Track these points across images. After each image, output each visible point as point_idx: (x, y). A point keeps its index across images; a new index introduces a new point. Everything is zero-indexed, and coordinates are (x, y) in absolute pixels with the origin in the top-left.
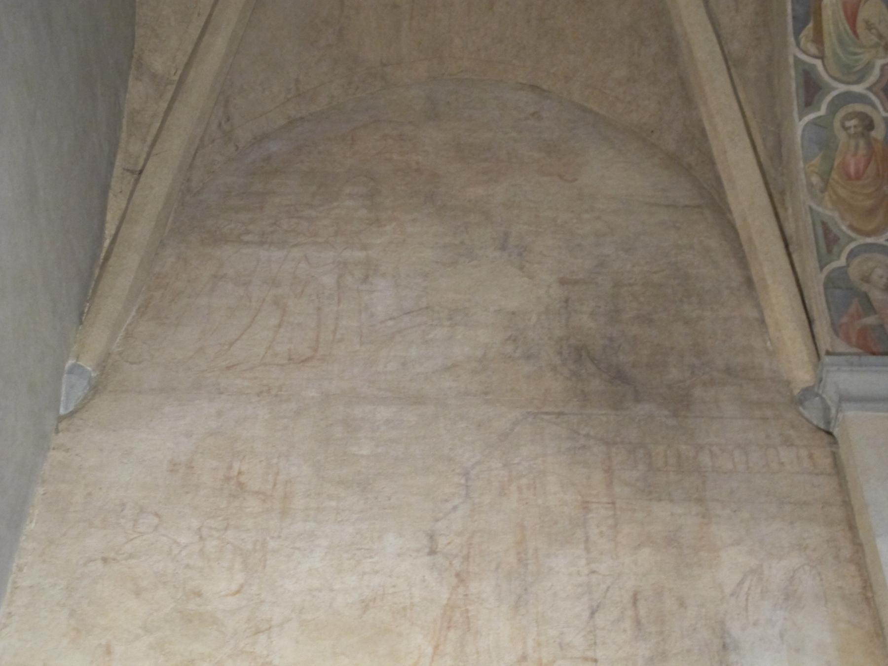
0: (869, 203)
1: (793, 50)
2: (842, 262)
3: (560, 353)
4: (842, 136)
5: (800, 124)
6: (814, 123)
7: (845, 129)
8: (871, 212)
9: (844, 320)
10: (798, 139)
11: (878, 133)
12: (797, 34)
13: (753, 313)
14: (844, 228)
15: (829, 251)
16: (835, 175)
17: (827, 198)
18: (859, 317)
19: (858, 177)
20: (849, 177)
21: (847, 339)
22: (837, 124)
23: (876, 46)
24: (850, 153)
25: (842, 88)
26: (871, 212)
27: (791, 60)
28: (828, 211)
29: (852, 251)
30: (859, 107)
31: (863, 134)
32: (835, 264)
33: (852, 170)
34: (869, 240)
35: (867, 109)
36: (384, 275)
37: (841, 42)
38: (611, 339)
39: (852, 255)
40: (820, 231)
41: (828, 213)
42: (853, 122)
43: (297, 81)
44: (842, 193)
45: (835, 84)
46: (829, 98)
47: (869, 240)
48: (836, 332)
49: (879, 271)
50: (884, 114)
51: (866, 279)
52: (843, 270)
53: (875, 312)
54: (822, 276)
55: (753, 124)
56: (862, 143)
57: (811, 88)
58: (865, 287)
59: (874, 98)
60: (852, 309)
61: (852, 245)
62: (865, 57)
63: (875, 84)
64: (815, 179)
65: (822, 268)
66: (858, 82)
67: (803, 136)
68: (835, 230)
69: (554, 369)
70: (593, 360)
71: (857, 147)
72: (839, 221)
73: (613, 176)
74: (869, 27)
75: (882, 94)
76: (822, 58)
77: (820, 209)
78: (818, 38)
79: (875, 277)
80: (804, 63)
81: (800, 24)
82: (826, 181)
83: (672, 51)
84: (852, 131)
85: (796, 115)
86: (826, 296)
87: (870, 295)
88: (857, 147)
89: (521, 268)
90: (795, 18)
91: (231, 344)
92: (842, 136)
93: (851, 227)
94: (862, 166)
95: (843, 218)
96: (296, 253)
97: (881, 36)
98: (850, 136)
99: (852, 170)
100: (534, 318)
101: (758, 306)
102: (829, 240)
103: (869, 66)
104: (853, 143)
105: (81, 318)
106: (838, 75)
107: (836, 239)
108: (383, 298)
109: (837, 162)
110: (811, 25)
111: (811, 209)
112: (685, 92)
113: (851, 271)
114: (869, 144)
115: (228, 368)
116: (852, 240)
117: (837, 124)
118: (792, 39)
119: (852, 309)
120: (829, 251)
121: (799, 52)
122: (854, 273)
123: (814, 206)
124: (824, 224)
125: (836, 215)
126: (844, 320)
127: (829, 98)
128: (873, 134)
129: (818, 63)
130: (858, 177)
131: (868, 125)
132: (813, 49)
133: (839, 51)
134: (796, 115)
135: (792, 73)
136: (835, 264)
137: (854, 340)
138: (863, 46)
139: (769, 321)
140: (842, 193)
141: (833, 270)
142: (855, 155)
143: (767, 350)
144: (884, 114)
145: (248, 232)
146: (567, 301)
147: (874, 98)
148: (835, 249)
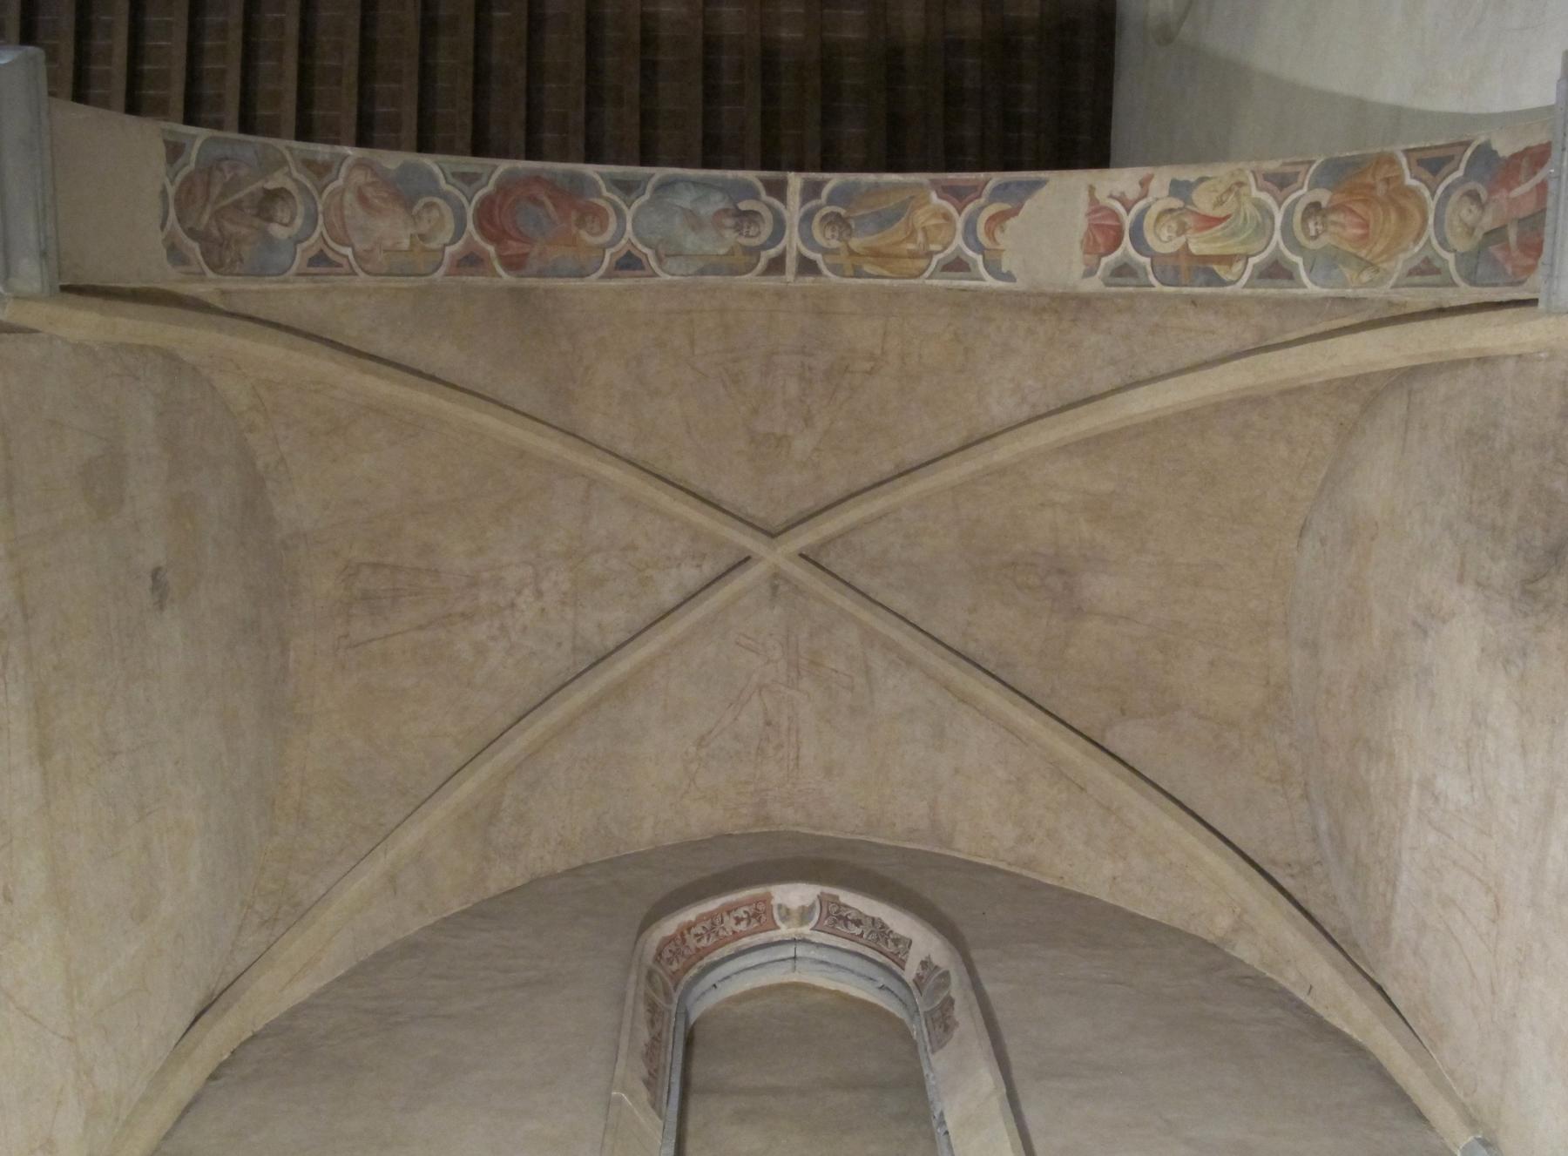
0: (1393, 216)
1: (1238, 289)
2: (1450, 257)
3: (1526, 615)
4: (1325, 240)
5: (1311, 288)
6: (1310, 271)
7: (1316, 237)
8: (1403, 213)
9: (1509, 270)
10: (1325, 291)
11: (1324, 196)
12: (1223, 283)
13: (1511, 364)
14: (1417, 249)
15: (1438, 271)
16: (1363, 253)
17: (1385, 265)
18: (1507, 248)
19: (1366, 225)
20: (1365, 237)
21: (1530, 269)
22: (1312, 245)
23: (1238, 195)
24: (1341, 232)
25: (1277, 236)
26: (1403, 213)
27: (1248, 291)
28: (1399, 266)
29: (1441, 244)
30: (1298, 217)
31: (1324, 216)
32: (1452, 267)
33: (1359, 232)
34: (1431, 221)
35: (1300, 208)
36: (1435, 776)
37: (1233, 234)
38: (1519, 547)
39: (1444, 243)
40: (1417, 279)
41: (1400, 266)
42: (1311, 225)
43: (1269, 780)
44: (1378, 248)
45: (1273, 244)
46: (1287, 253)
47: (1431, 221)
48: (1520, 283)
49: (1464, 212)
50: (1305, 189)
51: (1471, 231)
52: (1461, 258)
53: (1504, 227)
54: (1463, 285)
55: (1323, 326)
56: (1333, 217)
57: (1276, 271)
58: (1479, 234)
59: (1289, 201)
60: (1500, 255)
61: (1435, 242)
62: (1249, 209)
63: (1275, 198)
64: (1365, 277)
65: (1454, 284)
66: (1272, 218)
67: (1323, 286)
68: (1416, 262)
69: (1539, 629)
70: (1535, 580)
71: (1334, 223)
72: (1408, 255)
73: (1380, 479)
74: (1220, 203)
75: (1286, 191)
76: (1248, 257)
77: (1395, 276)
78: (1228, 260)
79: (1469, 218)
80: (1251, 277)
81: (1215, 280)
82: (1369, 265)
83: (1254, 401)
84: (1320, 227)
85: (1300, 292)
86: (1483, 285)
87: (1487, 228)
88: (1334, 223)
89: (1444, 622)
90: (1208, 284)
91: (1474, 976)
92: (1325, 240)
93: (1416, 241)
94: (1356, 220)
95: (1405, 250)
96: (1406, 857)
97: (1230, 190)
98: (1324, 231)
99: (1359, 232)
100: (1490, 630)
101: (1506, 357)
102: (1426, 269)
103: (1259, 205)
104: (1332, 228)
105: (1420, 1116)
106: (1264, 241)
107: (1427, 261)
108: (1452, 786)
109: (1346, 247)
110: (1215, 267)
111: (1395, 286)
112: (1294, 393)
113: (1460, 249)
114: (1335, 209)
115: (1493, 993)
116: (1429, 241)
117: (1312, 245)
118: (1228, 289)
119: (1500, 255)
120: (1438, 271)
121: (1239, 281)
122: (1463, 245)
123: (1391, 283)
124: (1410, 274)
125: (1402, 256)
126: (1509, 270)
127: (1287, 253)
128: (1324, 204)
129: (1253, 261)
130: (1366, 225)
131: (1314, 208)
132: (1238, 267)
133: (1243, 237)
134: (1300, 292)
135: (1260, 291)
136: (1452, 267)
137: (1530, 262)
138: (1238, 212)
139: (1516, 351)
140: (1378, 248)
141: (1458, 271)
142: (1343, 226)
143: (1548, 359)
144: (1305, 189)
145: (1384, 895)
146: (1478, 584)
147: (1289, 201)
148: (1437, 264)
